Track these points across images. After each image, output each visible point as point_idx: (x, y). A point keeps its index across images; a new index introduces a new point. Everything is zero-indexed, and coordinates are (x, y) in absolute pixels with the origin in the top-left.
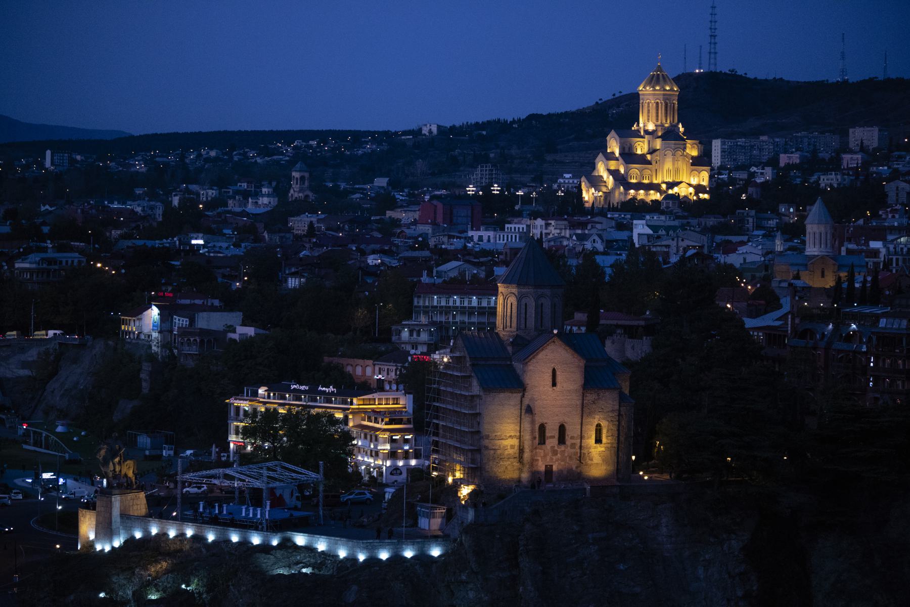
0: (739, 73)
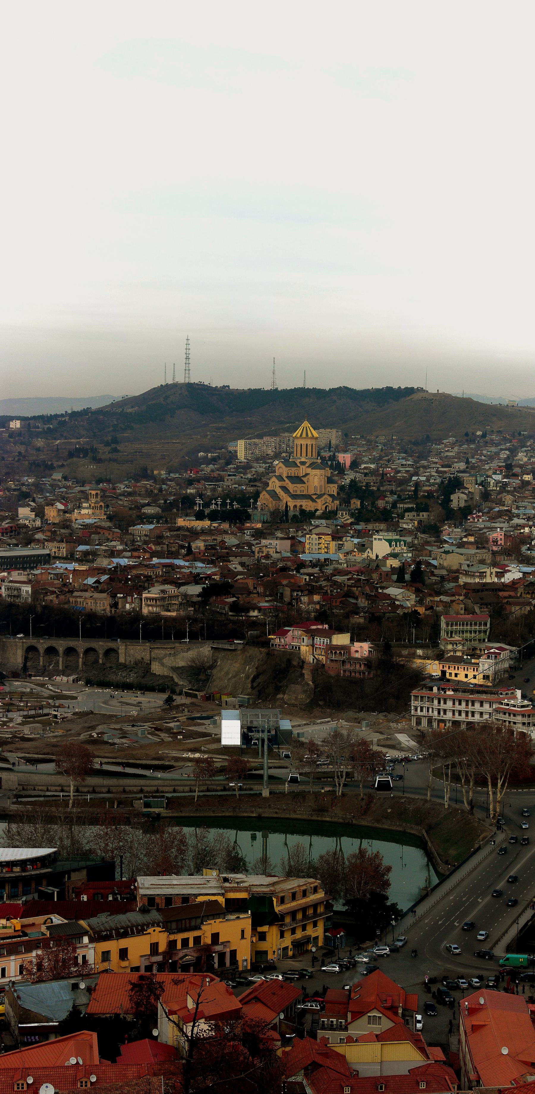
0: (205, 384)
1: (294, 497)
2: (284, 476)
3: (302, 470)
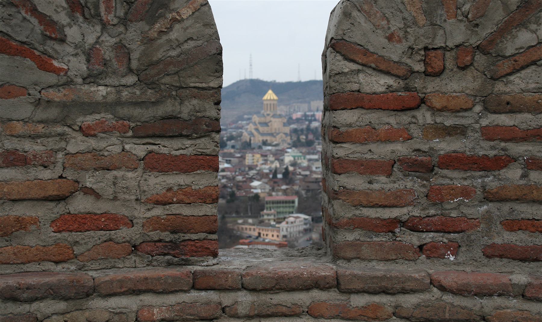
1: (263, 134)
2: (257, 122)
3: (268, 119)
